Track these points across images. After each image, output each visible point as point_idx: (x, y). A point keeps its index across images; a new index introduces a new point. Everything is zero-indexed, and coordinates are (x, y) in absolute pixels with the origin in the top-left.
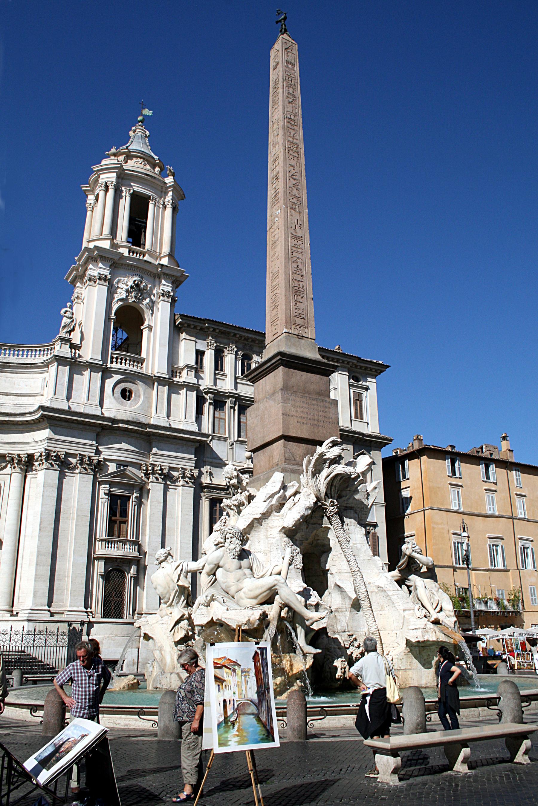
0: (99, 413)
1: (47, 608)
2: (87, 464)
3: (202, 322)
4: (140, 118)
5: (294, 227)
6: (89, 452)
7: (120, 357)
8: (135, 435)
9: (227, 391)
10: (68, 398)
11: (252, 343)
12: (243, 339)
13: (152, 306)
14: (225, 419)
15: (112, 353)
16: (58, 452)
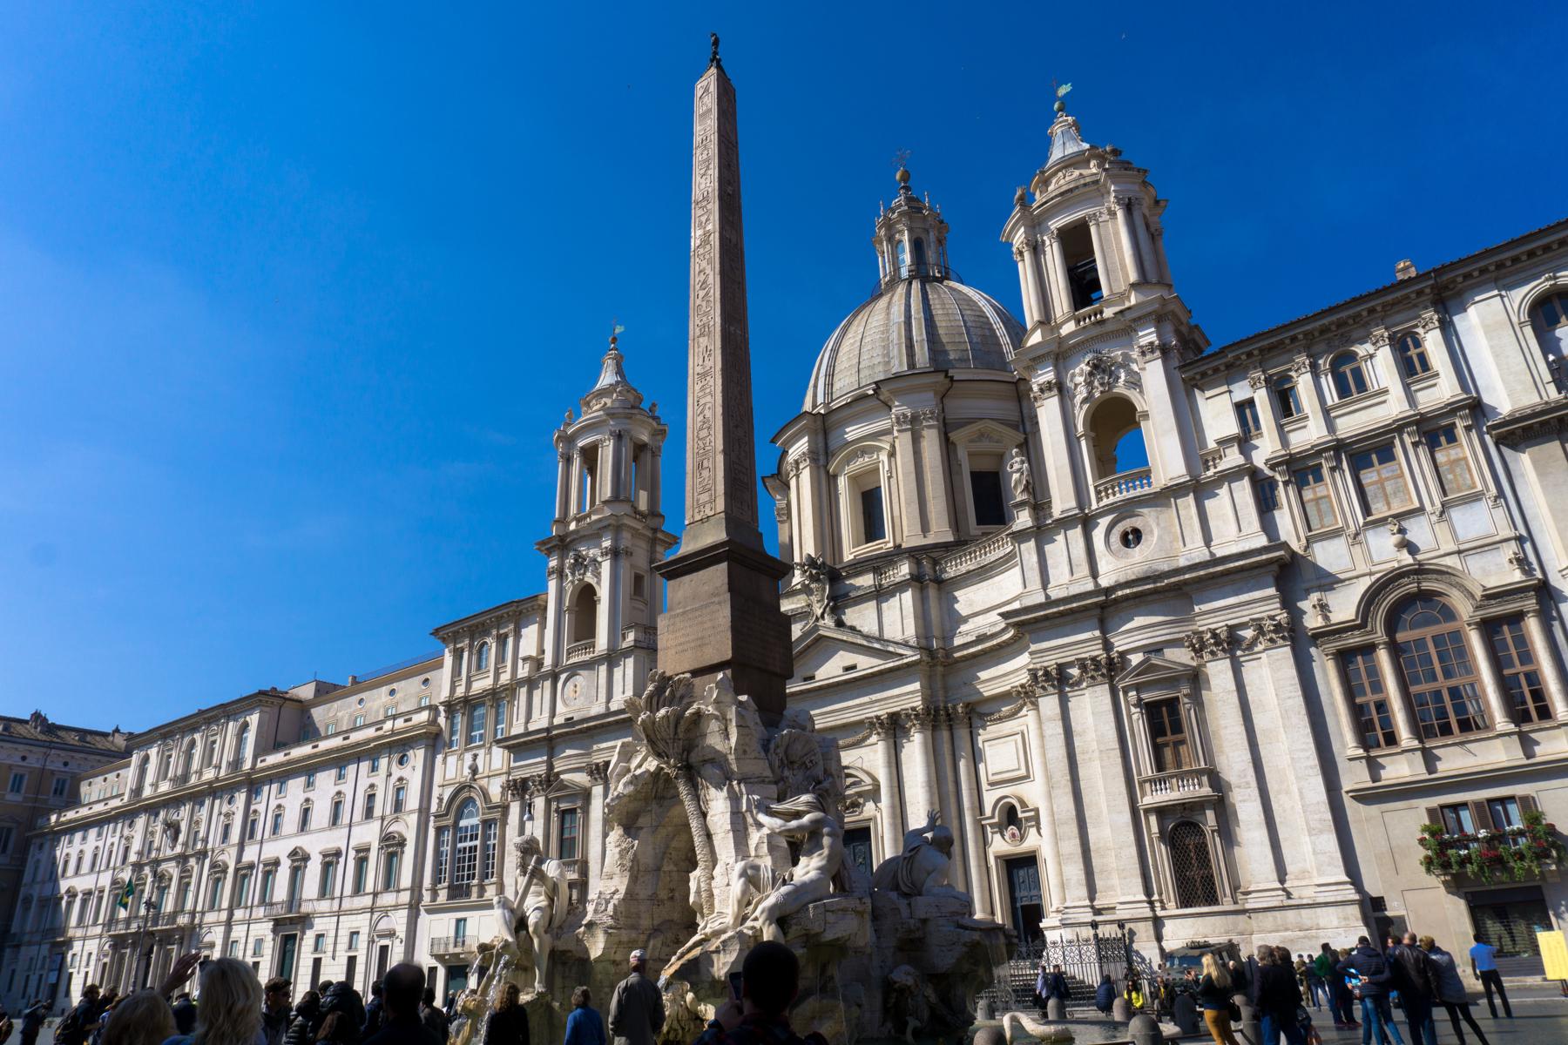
0: (1089, 586)
1: (1279, 886)
2: (1094, 670)
3: (1220, 356)
4: (1056, 106)
5: (701, 360)
6: (1096, 651)
7: (1109, 485)
8: (1156, 597)
9: (1390, 421)
10: (1208, 540)
11: (1340, 331)
12: (1316, 334)
13: (1135, 383)
14: (1328, 497)
15: (1096, 487)
16: (1045, 668)
